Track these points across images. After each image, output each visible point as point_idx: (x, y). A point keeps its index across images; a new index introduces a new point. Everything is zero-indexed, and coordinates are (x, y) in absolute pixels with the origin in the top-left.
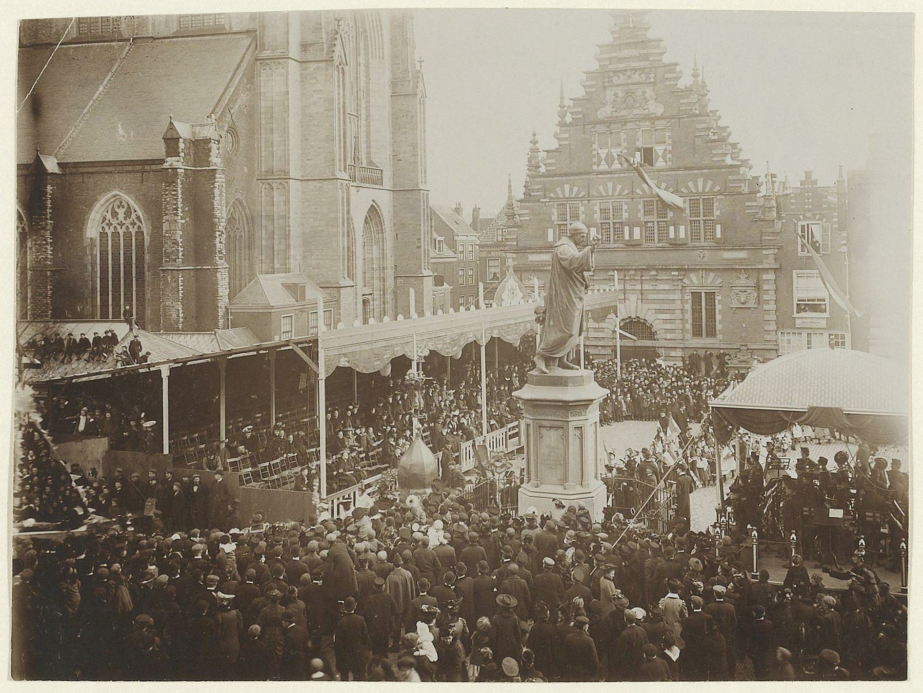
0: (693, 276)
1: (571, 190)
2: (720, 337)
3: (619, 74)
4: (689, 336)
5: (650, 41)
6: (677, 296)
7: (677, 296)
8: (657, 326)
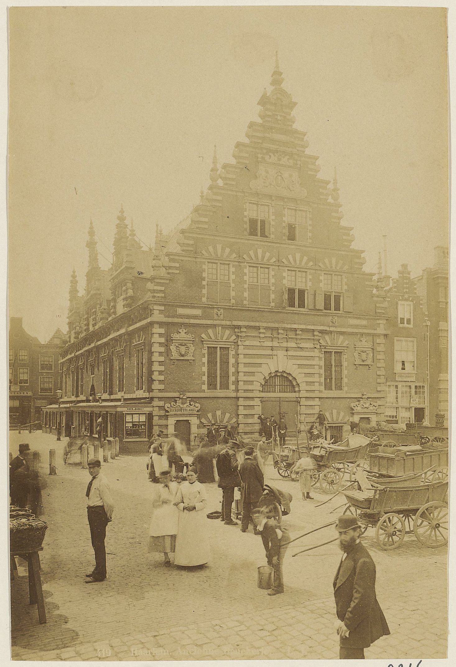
0: (327, 337)
1: (223, 249)
2: (345, 389)
3: (270, 154)
4: (322, 388)
5: (296, 132)
6: (316, 353)
7: (316, 353)
8: (300, 379)
